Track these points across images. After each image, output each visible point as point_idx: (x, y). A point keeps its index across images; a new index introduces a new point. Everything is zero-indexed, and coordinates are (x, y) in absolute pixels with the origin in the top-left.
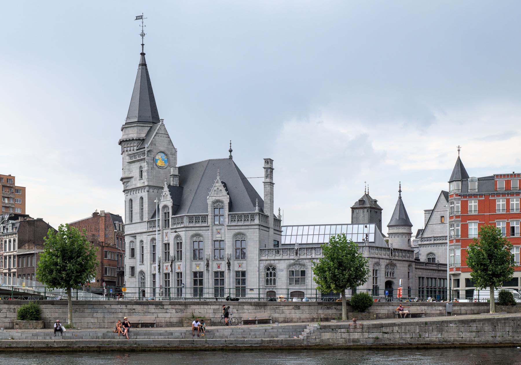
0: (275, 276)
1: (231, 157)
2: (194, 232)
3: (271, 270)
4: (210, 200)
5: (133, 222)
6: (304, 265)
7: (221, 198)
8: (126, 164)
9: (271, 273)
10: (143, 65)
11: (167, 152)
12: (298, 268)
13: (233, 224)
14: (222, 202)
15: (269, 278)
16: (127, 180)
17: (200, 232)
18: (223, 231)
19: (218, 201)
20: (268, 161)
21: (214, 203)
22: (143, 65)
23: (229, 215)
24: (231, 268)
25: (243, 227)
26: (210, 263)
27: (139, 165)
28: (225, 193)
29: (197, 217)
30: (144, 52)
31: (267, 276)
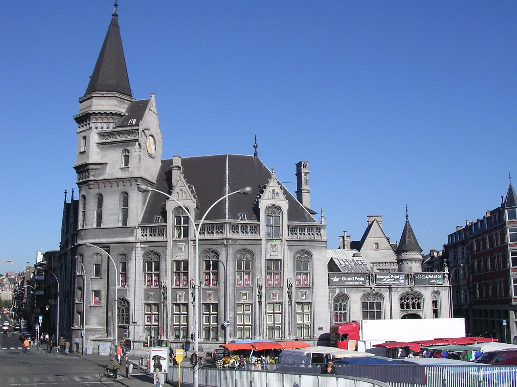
0: (345, 309)
1: (256, 154)
2: (239, 247)
3: (340, 302)
4: (263, 204)
5: (102, 226)
6: (381, 296)
7: (278, 203)
8: (95, 144)
9: (341, 305)
10: (114, 26)
11: (155, 137)
12: (371, 299)
13: (295, 237)
14: (279, 208)
15: (339, 312)
16: (95, 167)
17: (249, 247)
18: (279, 247)
19: (274, 206)
20: (299, 165)
21: (268, 208)
22: (114, 26)
23: (289, 226)
24: (293, 299)
25: (307, 244)
26: (264, 291)
27: (122, 149)
28: (282, 196)
29: (244, 227)
30: (117, 13)
31: (336, 309)
